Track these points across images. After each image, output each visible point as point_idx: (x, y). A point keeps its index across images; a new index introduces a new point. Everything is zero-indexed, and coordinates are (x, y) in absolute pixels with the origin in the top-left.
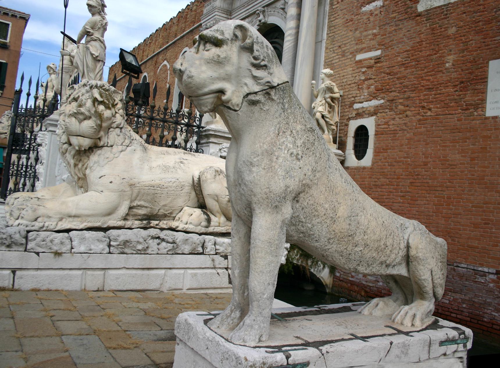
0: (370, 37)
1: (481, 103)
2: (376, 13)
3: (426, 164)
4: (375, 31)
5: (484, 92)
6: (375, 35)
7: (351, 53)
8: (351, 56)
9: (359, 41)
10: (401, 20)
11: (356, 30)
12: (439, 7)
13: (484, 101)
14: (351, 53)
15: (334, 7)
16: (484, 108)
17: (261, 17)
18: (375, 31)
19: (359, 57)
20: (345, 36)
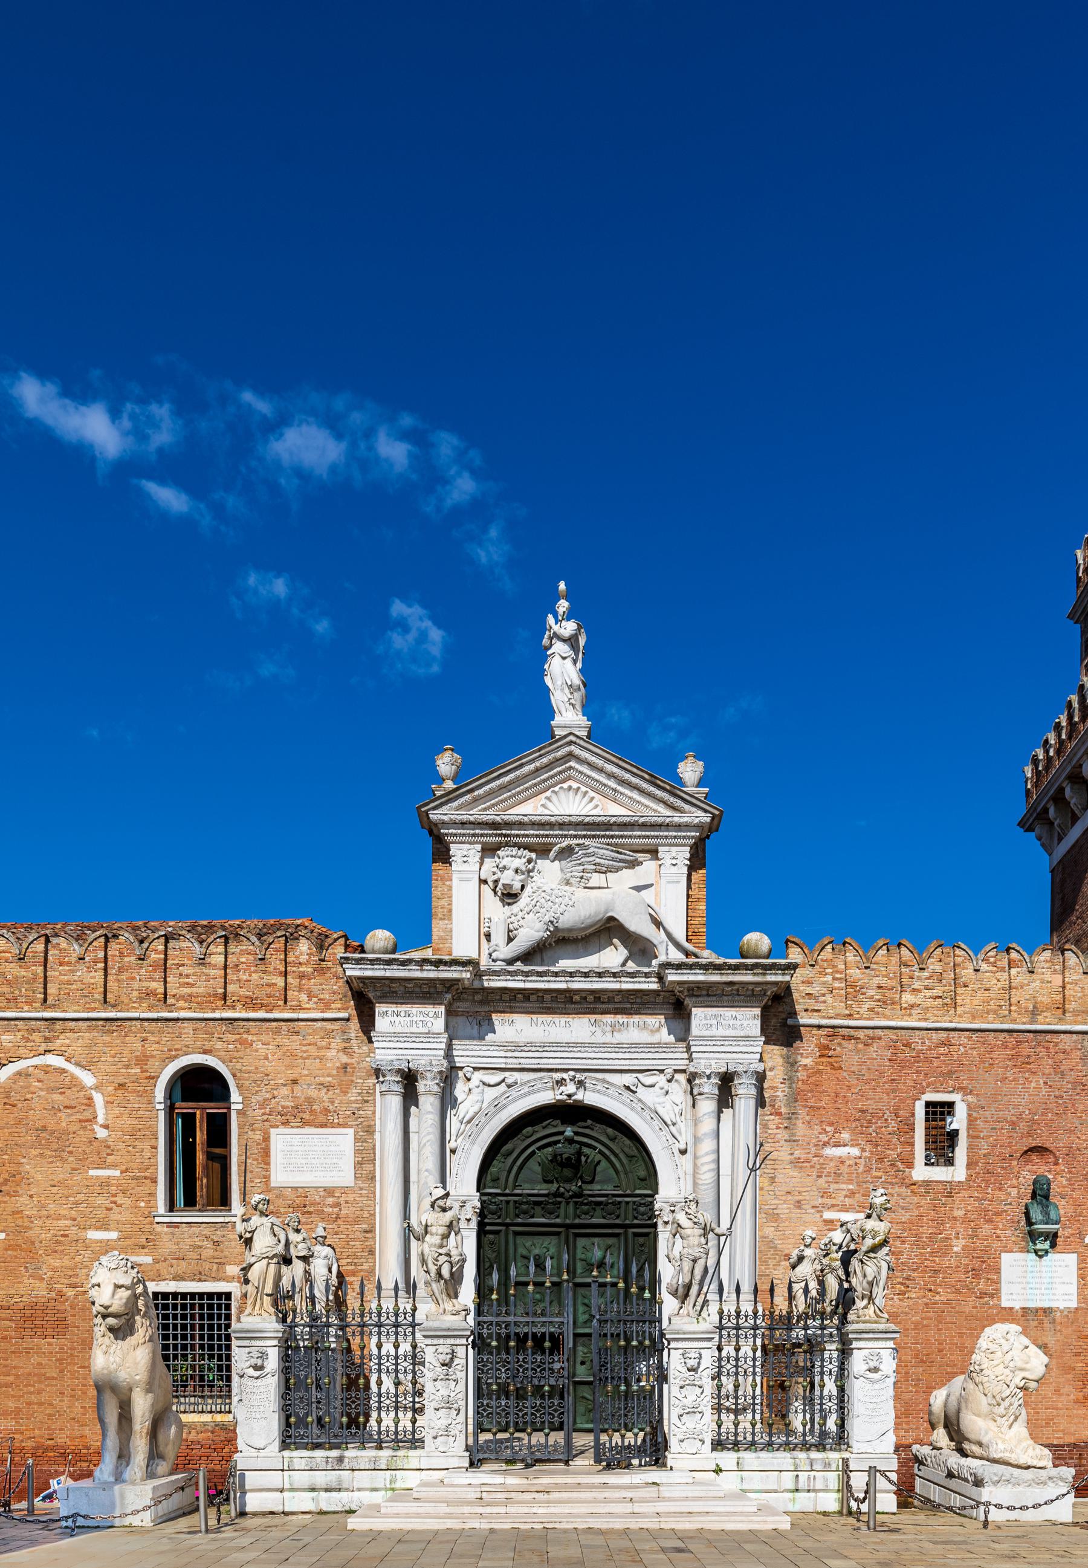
0: (844, 1193)
1: (996, 1294)
2: (851, 1162)
3: (940, 1351)
4: (851, 1187)
5: (998, 1282)
6: (852, 1193)
7: (813, 1207)
8: (813, 1211)
9: (825, 1194)
10: (891, 1183)
11: (819, 1177)
12: (940, 1182)
13: (998, 1291)
14: (813, 1207)
15: (770, 1132)
16: (999, 1298)
17: (571, 1088)
18: (851, 1187)
19: (828, 1215)
20: (797, 1180)
